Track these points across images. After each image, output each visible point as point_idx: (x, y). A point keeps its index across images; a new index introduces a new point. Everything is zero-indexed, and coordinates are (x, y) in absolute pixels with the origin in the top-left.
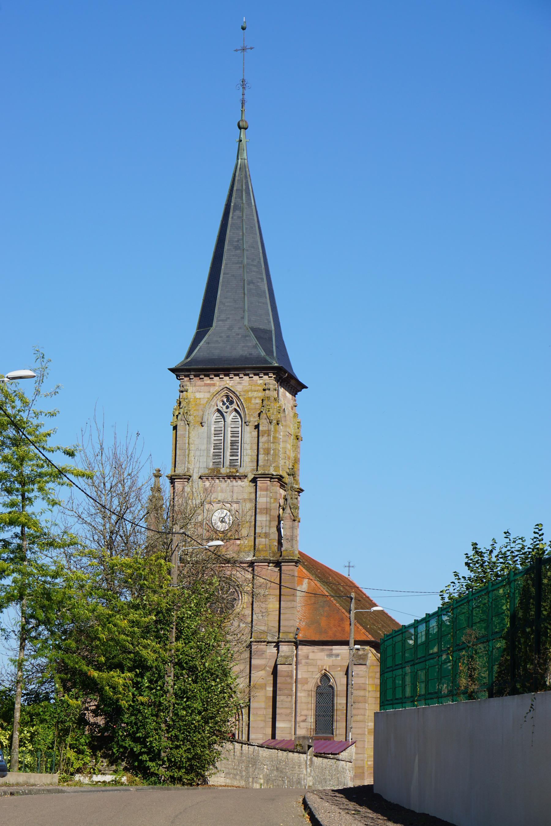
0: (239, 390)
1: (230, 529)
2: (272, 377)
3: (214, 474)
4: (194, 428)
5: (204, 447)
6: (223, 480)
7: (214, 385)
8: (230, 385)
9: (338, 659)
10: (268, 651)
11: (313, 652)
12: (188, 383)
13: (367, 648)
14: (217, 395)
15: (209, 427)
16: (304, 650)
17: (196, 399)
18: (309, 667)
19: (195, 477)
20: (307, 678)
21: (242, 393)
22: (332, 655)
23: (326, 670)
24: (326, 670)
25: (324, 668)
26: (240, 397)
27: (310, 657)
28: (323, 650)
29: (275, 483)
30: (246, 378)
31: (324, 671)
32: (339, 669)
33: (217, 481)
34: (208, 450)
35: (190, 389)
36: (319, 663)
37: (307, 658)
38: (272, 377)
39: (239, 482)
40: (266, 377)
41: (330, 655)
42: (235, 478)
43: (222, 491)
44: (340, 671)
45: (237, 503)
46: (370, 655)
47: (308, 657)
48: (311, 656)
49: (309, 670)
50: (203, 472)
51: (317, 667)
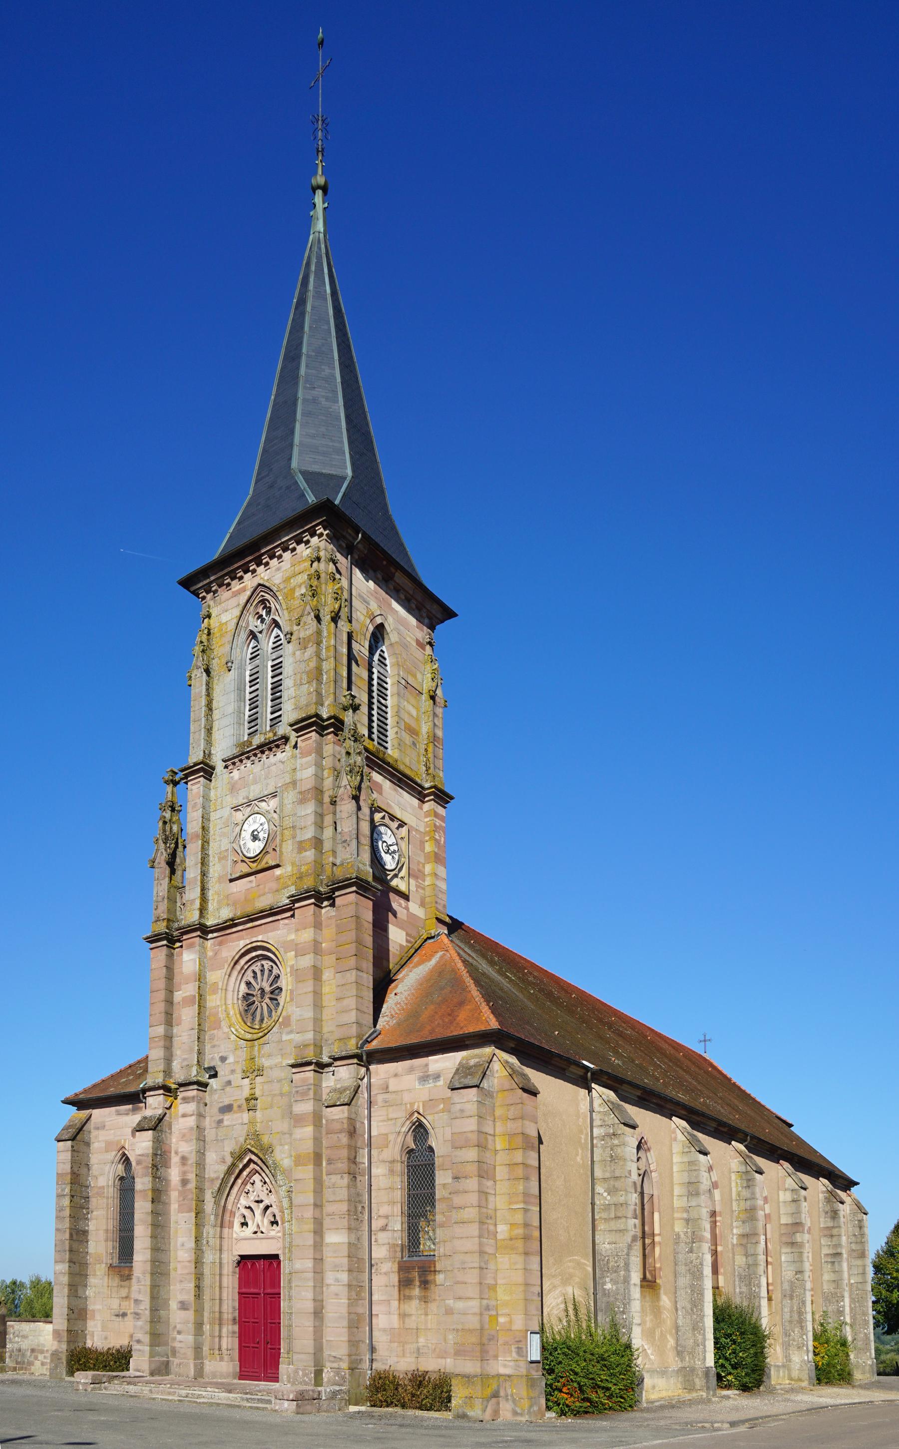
0: (277, 582)
1: (264, 852)
2: (321, 535)
3: (243, 754)
4: (218, 680)
5: (231, 708)
6: (256, 760)
7: (244, 590)
8: (266, 578)
9: (439, 1084)
10: (324, 1085)
11: (396, 1075)
12: (211, 603)
13: (488, 1050)
14: (249, 605)
15: (242, 669)
16: (381, 1071)
17: (221, 624)
18: (391, 1109)
19: (220, 766)
20: (386, 1135)
21: (282, 587)
22: (428, 1076)
23: (419, 1113)
24: (419, 1113)
25: (415, 1108)
26: (277, 594)
27: (391, 1089)
28: (411, 1070)
29: (330, 736)
30: (287, 555)
31: (416, 1115)
32: (442, 1106)
33: (249, 763)
34: (240, 712)
35: (214, 612)
36: (407, 1098)
37: (386, 1089)
38: (321, 535)
39: (280, 756)
40: (315, 540)
41: (424, 1079)
42: (270, 749)
43: (255, 782)
44: (443, 1111)
45: (274, 795)
46: (496, 1066)
47: (387, 1087)
48: (393, 1085)
49: (391, 1116)
50: (228, 754)
51: (404, 1108)
